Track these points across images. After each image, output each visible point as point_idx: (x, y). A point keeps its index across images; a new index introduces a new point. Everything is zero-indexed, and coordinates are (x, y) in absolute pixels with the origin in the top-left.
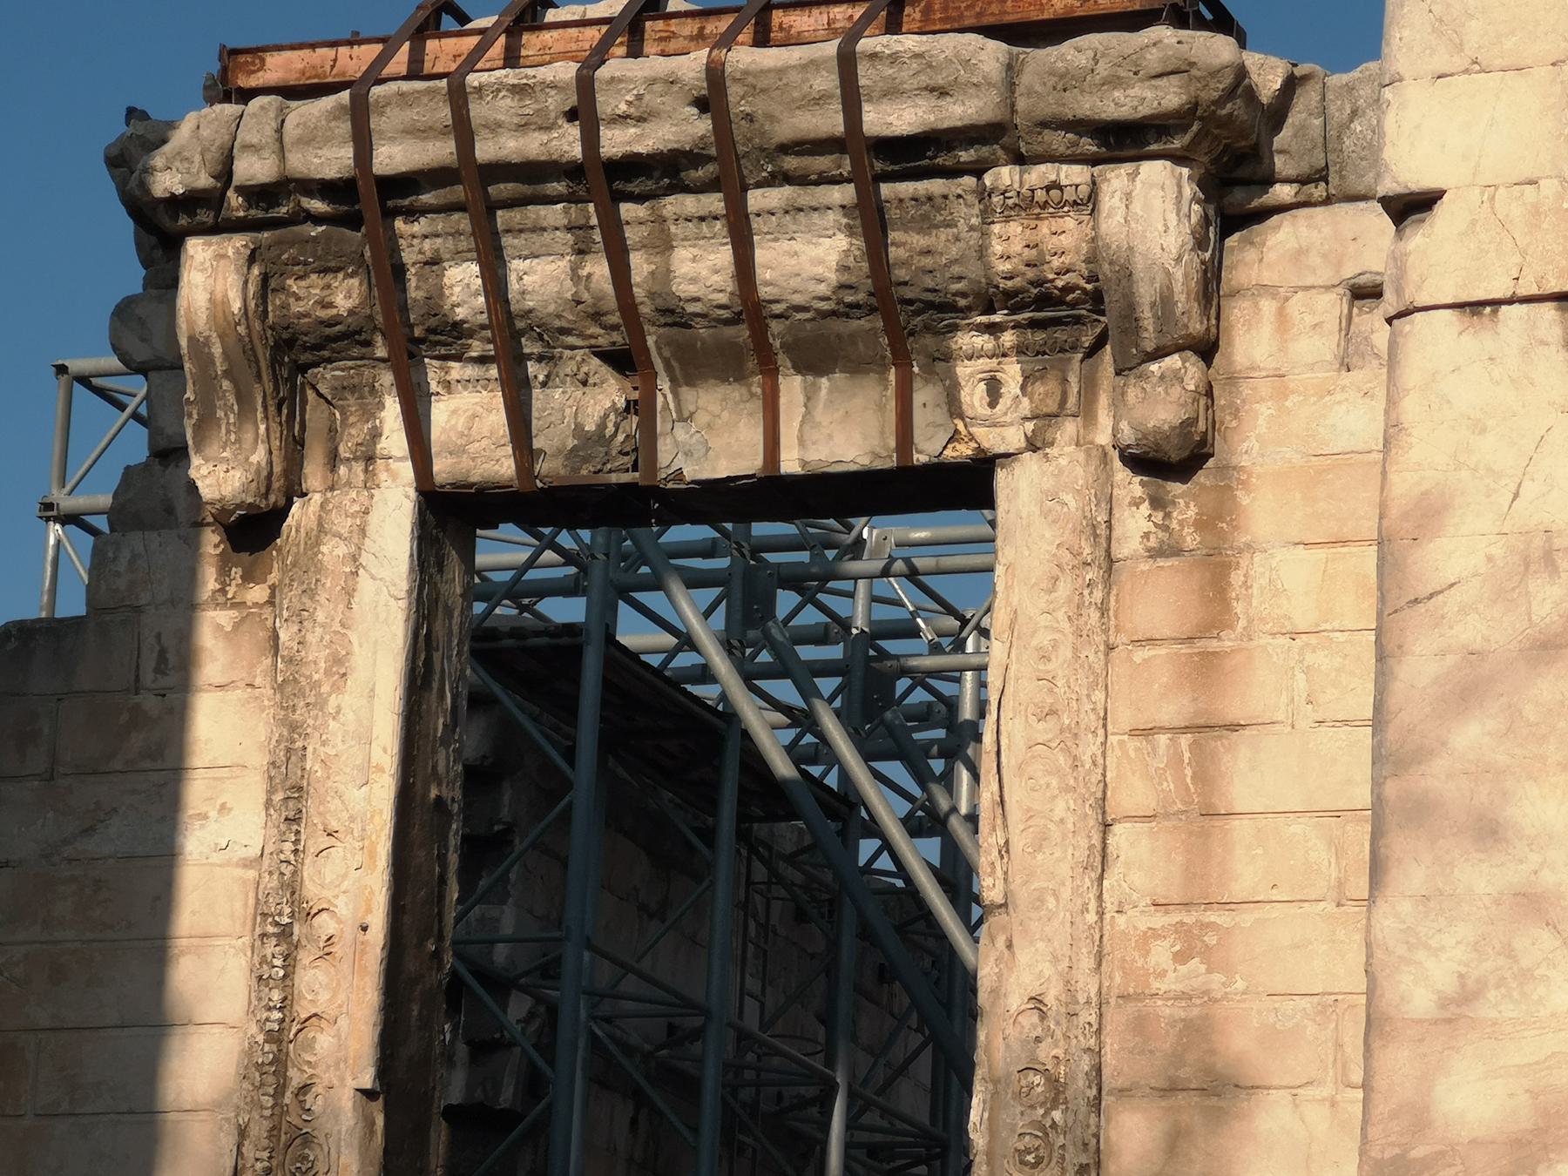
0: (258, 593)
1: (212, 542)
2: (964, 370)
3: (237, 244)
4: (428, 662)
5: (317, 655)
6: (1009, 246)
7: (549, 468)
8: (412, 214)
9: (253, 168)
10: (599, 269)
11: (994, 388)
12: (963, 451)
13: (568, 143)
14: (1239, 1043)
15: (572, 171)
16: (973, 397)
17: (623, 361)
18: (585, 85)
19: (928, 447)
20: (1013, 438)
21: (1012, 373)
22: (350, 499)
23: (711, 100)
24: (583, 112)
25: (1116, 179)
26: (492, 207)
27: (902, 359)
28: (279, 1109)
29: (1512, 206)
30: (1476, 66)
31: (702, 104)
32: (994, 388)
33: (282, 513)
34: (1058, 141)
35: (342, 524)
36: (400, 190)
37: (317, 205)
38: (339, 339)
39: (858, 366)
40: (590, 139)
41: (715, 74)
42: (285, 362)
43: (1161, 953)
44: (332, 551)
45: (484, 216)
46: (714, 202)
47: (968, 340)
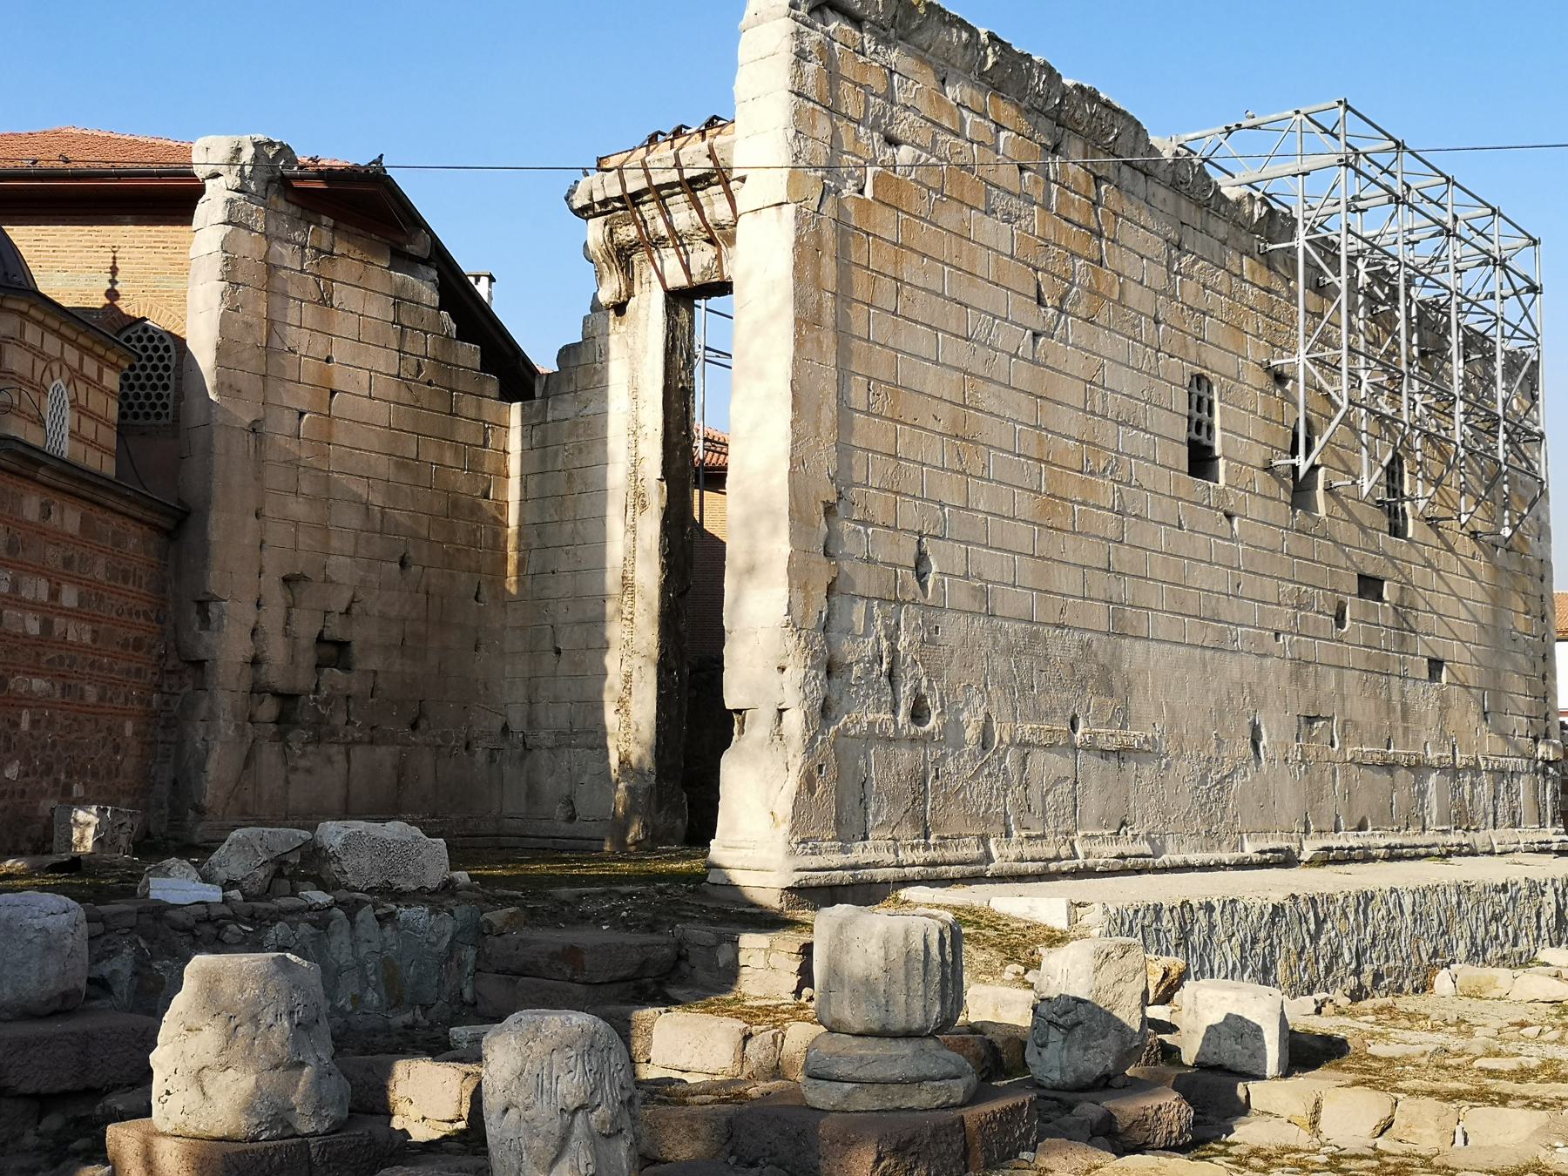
0: (623, 328)
1: (612, 313)
3: (601, 219)
4: (674, 345)
5: (639, 346)
7: (697, 279)
8: (644, 203)
9: (598, 197)
10: (694, 213)
13: (674, 176)
15: (679, 184)
17: (711, 241)
18: (677, 156)
22: (646, 296)
23: (711, 156)
24: (678, 166)
26: (663, 199)
28: (636, 487)
33: (625, 304)
35: (643, 304)
36: (636, 196)
37: (618, 205)
38: (634, 246)
40: (681, 174)
41: (711, 148)
42: (622, 256)
44: (642, 313)
45: (661, 201)
46: (720, 188)
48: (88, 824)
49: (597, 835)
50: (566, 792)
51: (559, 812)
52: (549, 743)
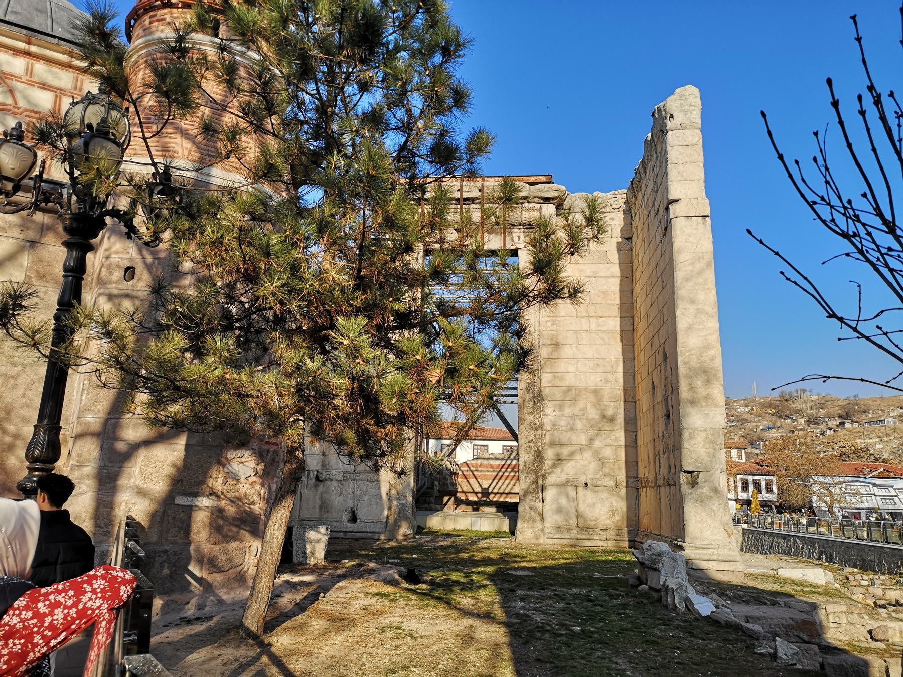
2: (514, 235)
6: (525, 216)
11: (519, 238)
12: (513, 247)
14: (560, 339)
16: (516, 239)
19: (509, 246)
20: (522, 246)
21: (522, 236)
25: (545, 206)
27: (504, 233)
29: (694, 202)
30: (686, 180)
31: (480, 190)
32: (519, 238)
34: (536, 200)
39: (497, 233)
40: (461, 194)
41: (483, 186)
43: (549, 324)
46: (478, 206)
47: (515, 230)
48: (318, 541)
49: (377, 530)
50: (350, 504)
51: (345, 517)
52: (339, 478)
